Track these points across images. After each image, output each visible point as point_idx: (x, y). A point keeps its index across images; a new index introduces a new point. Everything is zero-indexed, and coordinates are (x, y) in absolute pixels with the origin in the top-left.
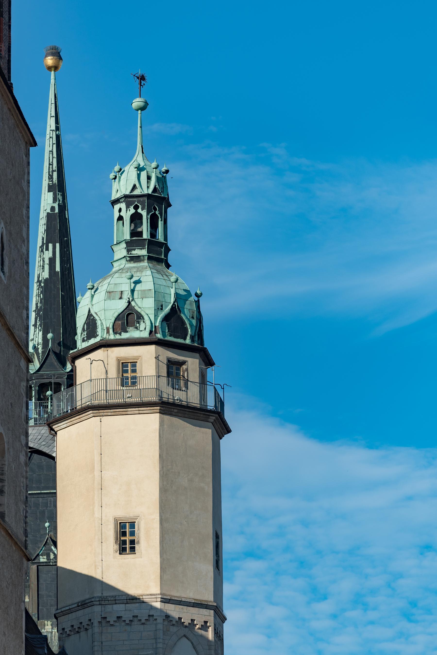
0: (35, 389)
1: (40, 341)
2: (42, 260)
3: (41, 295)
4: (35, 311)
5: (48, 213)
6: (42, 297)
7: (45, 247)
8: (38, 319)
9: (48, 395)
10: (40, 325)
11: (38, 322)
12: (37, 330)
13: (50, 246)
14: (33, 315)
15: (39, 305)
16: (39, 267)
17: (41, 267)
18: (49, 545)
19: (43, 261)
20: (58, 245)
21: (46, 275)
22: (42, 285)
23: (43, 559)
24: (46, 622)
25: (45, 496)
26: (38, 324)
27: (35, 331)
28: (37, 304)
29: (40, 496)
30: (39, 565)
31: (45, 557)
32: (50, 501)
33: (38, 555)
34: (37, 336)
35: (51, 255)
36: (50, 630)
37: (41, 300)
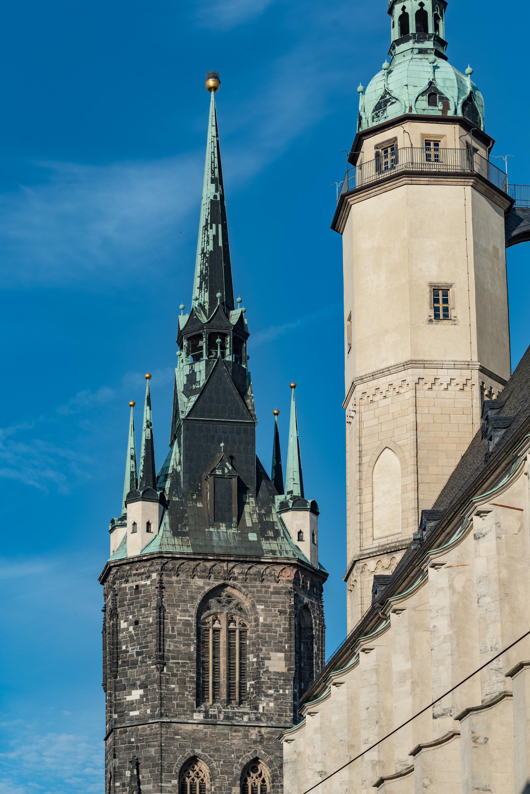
0: (206, 337)
1: (207, 299)
2: (206, 237)
3: (207, 264)
4: (200, 277)
5: (211, 200)
6: (207, 265)
7: (209, 226)
8: (204, 283)
9: (218, 342)
10: (205, 287)
11: (203, 285)
12: (203, 291)
13: (214, 226)
14: (197, 281)
15: (204, 272)
16: (203, 243)
17: (205, 242)
18: (224, 461)
19: (208, 237)
20: (220, 226)
21: (210, 248)
22: (207, 256)
23: (218, 472)
24: (221, 524)
25: (215, 423)
26: (203, 286)
27: (200, 293)
28: (201, 272)
29: (211, 423)
30: (216, 476)
31: (221, 471)
32: (220, 428)
33: (215, 469)
34: (203, 296)
35: (214, 233)
36: (225, 531)
37: (206, 269)
